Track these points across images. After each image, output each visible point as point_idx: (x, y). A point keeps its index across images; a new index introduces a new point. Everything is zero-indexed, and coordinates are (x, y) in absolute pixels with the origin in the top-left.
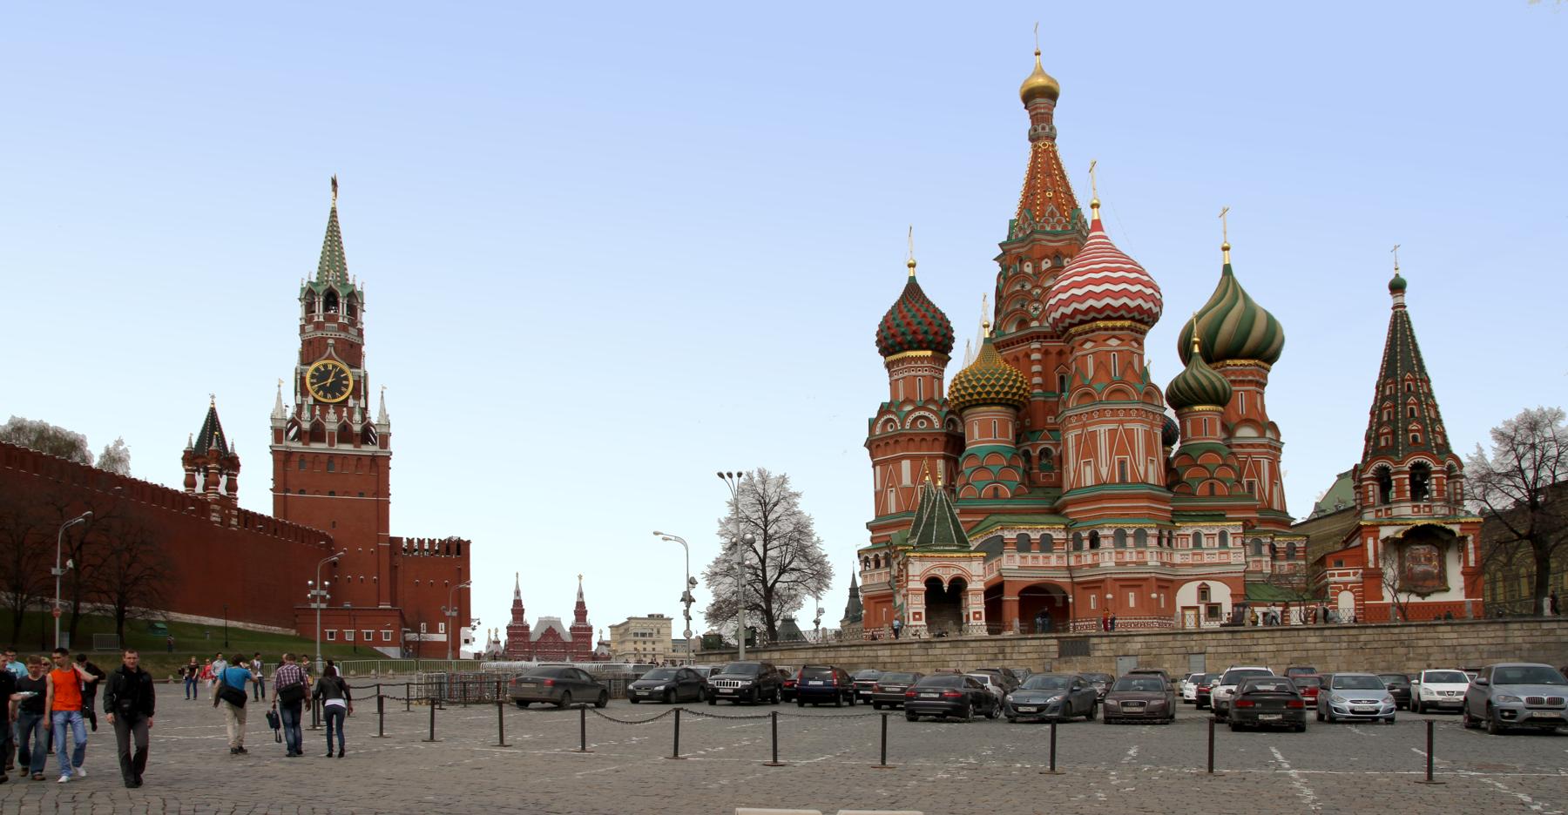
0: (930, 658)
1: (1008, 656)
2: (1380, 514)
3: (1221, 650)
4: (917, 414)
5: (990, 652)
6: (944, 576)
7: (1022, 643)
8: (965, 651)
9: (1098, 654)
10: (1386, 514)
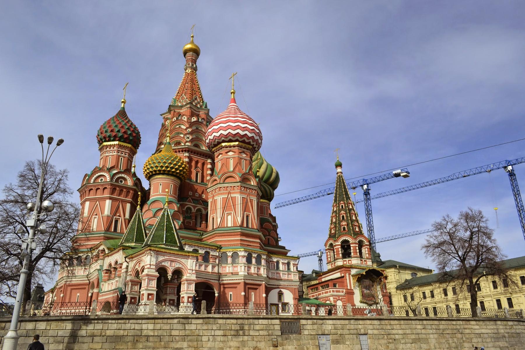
0: (187, 332)
1: (246, 333)
2: (345, 262)
3: (376, 332)
4: (120, 175)
5: (233, 328)
6: (170, 268)
7: (256, 322)
8: (215, 328)
9: (306, 332)
10: (349, 263)
